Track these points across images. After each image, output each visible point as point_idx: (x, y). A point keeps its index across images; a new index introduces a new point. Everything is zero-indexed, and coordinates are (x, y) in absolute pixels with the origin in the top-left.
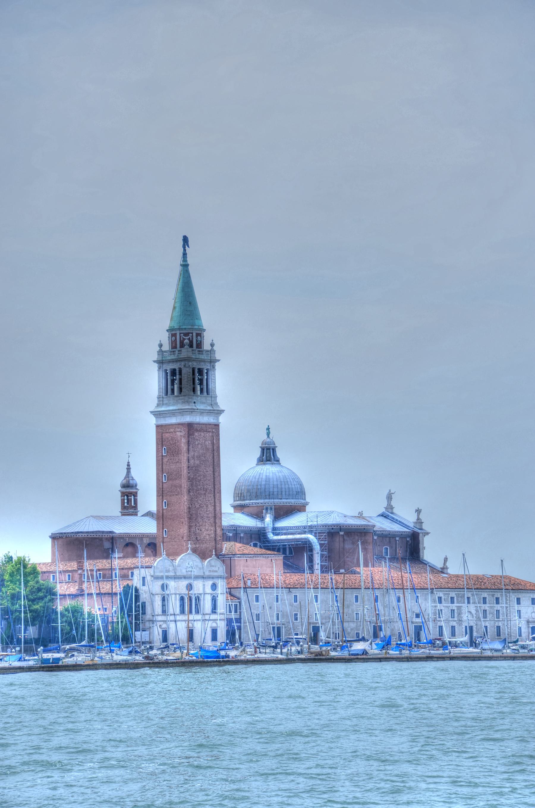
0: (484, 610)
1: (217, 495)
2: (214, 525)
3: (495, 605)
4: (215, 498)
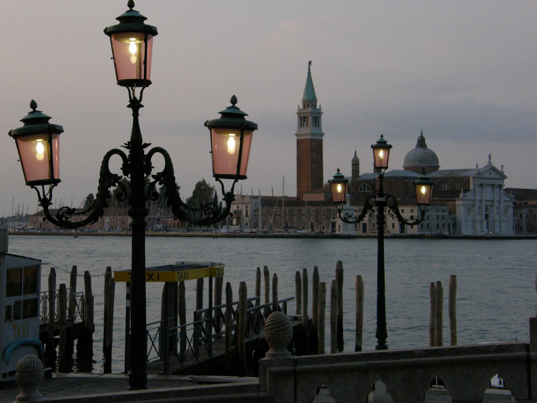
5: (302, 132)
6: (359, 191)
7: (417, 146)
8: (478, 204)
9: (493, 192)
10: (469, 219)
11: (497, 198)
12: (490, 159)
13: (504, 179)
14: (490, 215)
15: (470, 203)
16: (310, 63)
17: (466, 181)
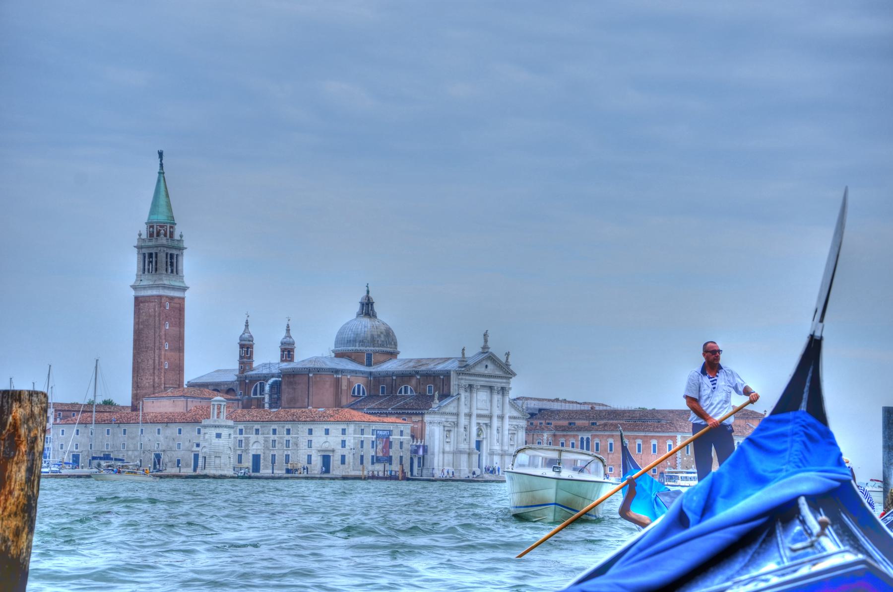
0: (273, 441)
1: (157, 351)
2: (153, 375)
3: (285, 435)
4: (154, 353)
5: (145, 283)
6: (252, 396)
7: (358, 315)
8: (463, 421)
9: (491, 401)
11: (497, 412)
12: (486, 341)
13: (511, 378)
14: (485, 442)
15: (450, 420)
17: (443, 379)
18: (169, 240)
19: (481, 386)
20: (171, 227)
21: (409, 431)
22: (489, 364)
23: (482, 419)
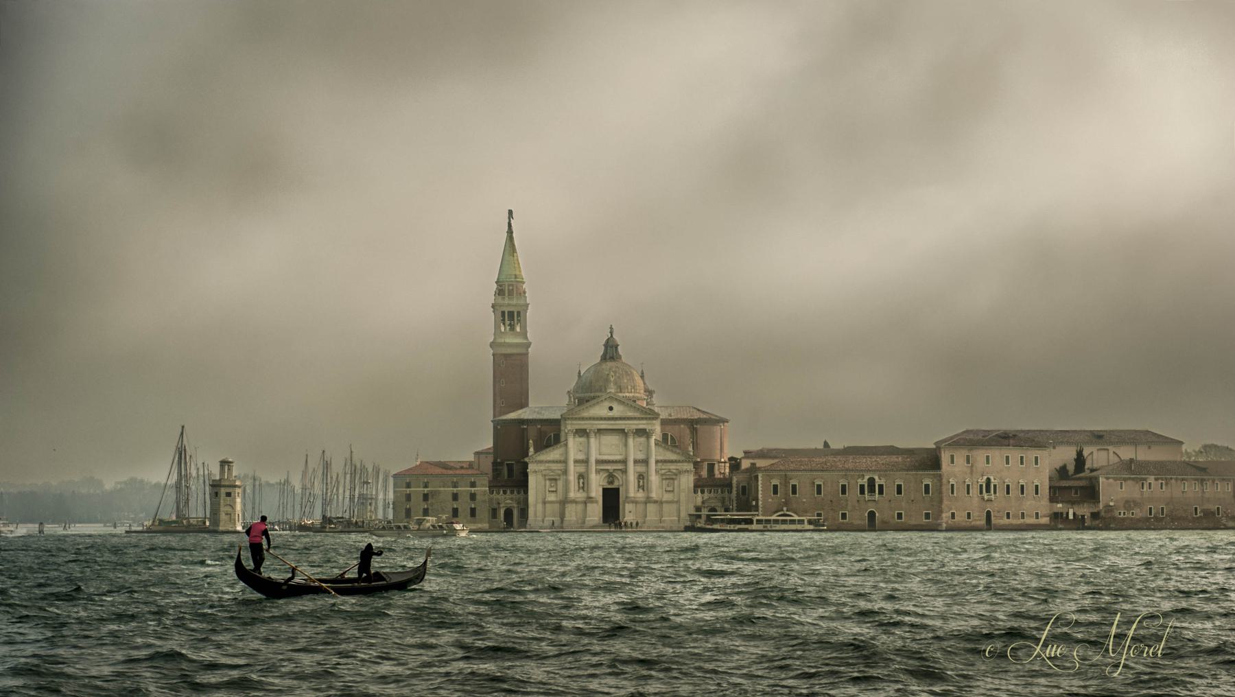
8: (573, 470)
9: (626, 445)
10: (552, 497)
16: (510, 212)
18: (507, 299)
19: (598, 430)
20: (509, 285)
21: (486, 482)
22: (615, 405)
23: (611, 464)
